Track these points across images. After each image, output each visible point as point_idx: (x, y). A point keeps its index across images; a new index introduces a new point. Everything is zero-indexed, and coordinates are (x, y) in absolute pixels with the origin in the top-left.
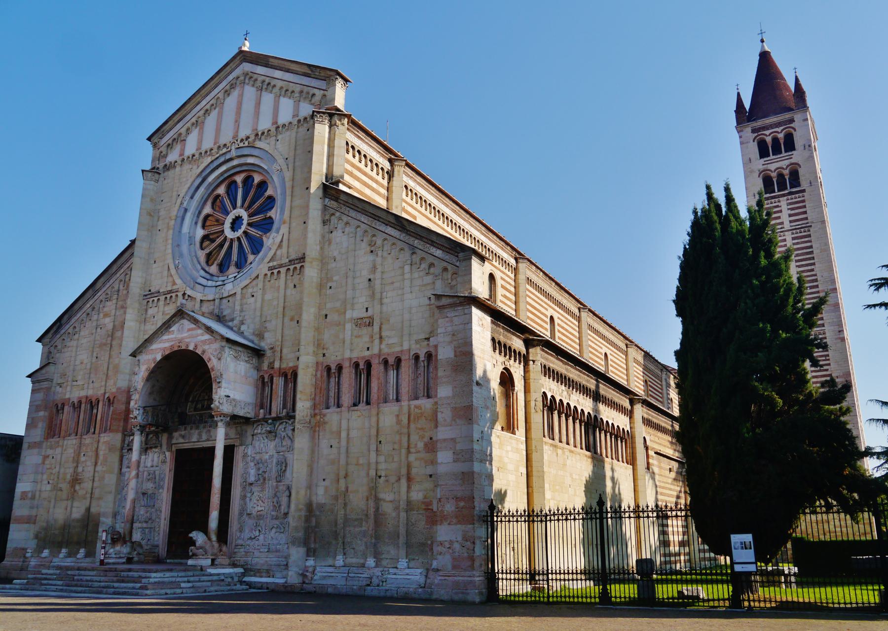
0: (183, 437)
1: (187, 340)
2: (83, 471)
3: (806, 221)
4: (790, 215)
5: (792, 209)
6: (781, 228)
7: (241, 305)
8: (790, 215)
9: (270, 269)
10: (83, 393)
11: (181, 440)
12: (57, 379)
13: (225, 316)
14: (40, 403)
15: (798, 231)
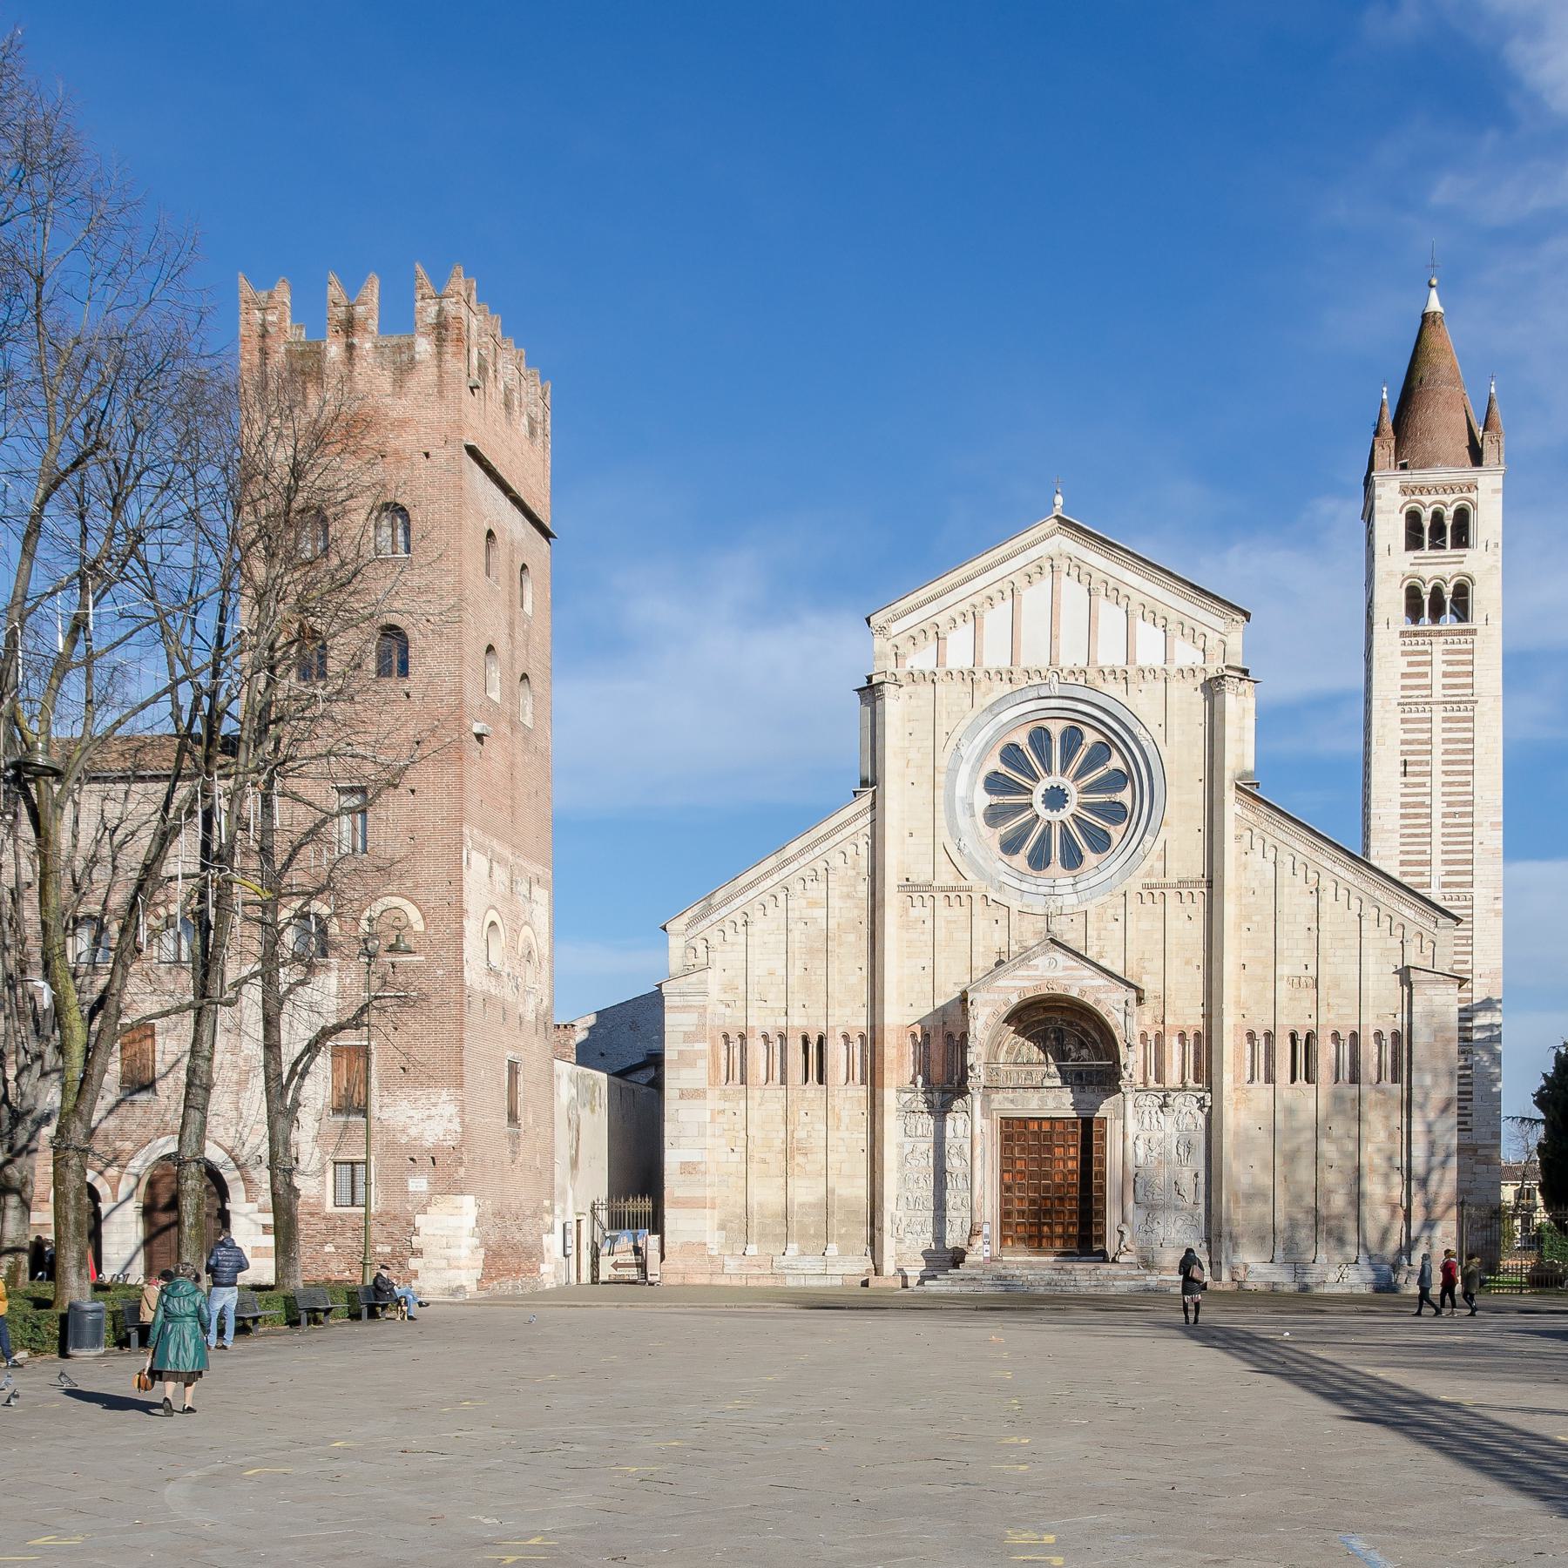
0: (1012, 1102)
1: (1064, 982)
2: (808, 1137)
3: (1470, 691)
4: (1445, 675)
5: (1449, 663)
6: (1426, 696)
7: (1099, 930)
8: (1445, 675)
9: (1146, 886)
10: (782, 1022)
11: (1012, 1107)
12: (715, 992)
13: (1066, 941)
14: (693, 1029)
15: (1455, 706)
